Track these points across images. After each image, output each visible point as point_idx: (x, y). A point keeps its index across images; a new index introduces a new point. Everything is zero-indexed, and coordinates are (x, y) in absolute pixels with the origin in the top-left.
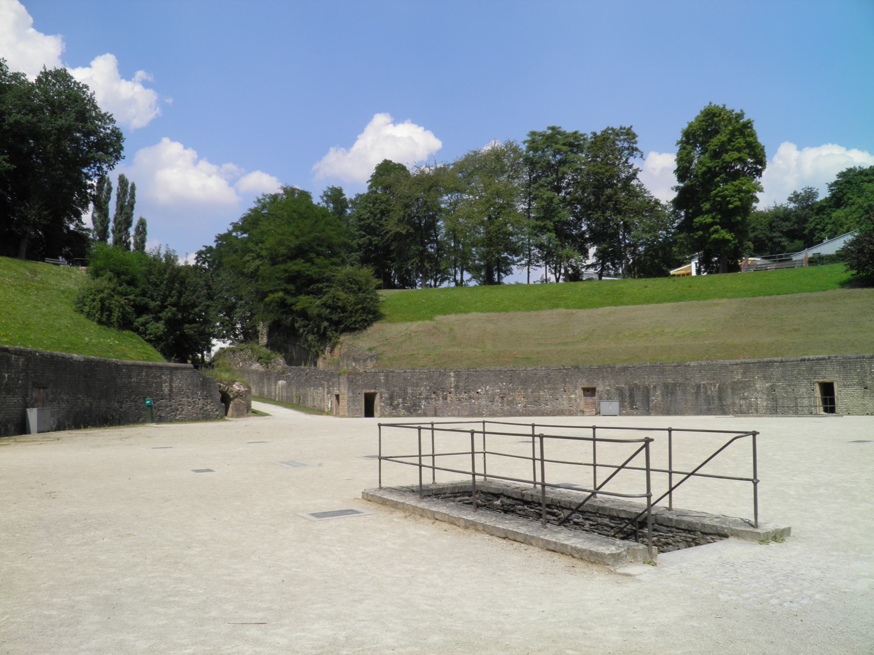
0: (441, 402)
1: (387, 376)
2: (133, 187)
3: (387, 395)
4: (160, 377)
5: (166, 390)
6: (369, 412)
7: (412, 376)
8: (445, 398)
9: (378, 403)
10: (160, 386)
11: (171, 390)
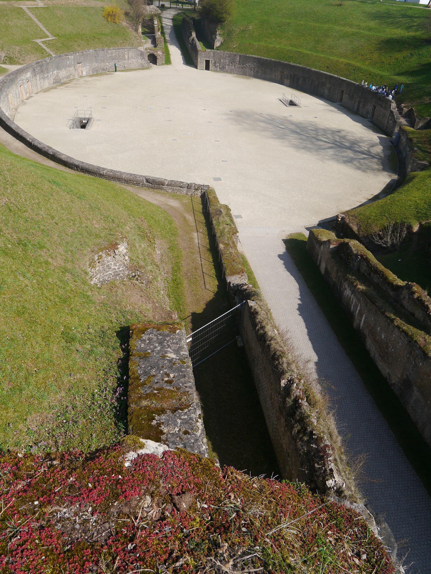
0: (233, 67)
1: (214, 54)
3: (213, 62)
4: (124, 53)
5: (127, 57)
6: (207, 68)
7: (223, 55)
8: (235, 66)
10: (124, 56)
11: (128, 57)
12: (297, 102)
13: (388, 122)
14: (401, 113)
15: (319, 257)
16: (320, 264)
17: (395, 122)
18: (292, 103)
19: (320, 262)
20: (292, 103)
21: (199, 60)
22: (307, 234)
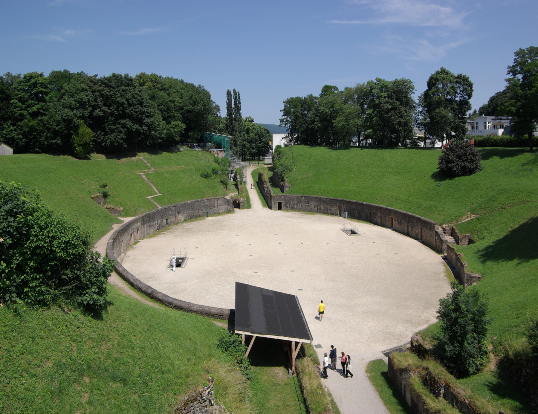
1: (284, 197)
2: (239, 94)
6: (280, 208)
9: (282, 206)
12: (356, 231)
13: (436, 242)
14: (445, 233)
15: (403, 387)
16: (405, 395)
17: (442, 241)
18: (353, 233)
19: (405, 393)
20: (353, 233)
21: (273, 203)
22: (386, 359)
